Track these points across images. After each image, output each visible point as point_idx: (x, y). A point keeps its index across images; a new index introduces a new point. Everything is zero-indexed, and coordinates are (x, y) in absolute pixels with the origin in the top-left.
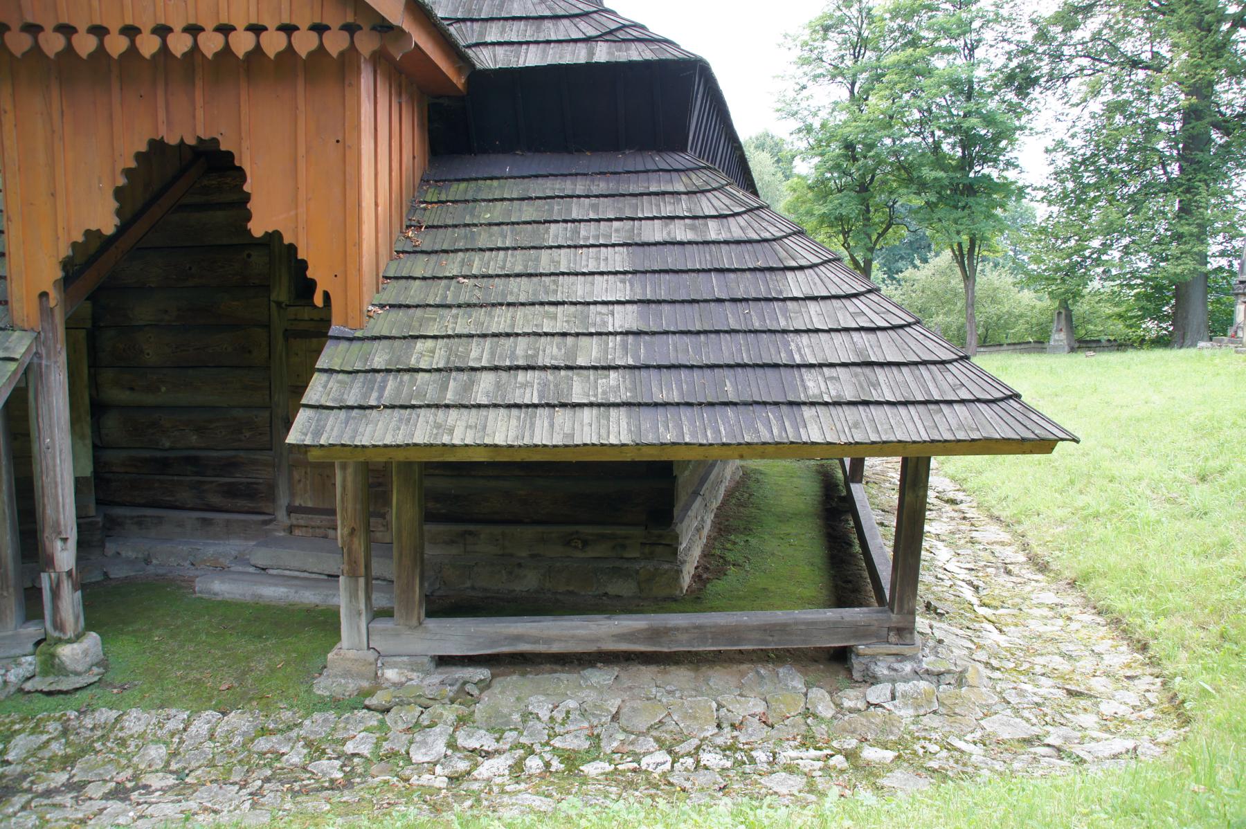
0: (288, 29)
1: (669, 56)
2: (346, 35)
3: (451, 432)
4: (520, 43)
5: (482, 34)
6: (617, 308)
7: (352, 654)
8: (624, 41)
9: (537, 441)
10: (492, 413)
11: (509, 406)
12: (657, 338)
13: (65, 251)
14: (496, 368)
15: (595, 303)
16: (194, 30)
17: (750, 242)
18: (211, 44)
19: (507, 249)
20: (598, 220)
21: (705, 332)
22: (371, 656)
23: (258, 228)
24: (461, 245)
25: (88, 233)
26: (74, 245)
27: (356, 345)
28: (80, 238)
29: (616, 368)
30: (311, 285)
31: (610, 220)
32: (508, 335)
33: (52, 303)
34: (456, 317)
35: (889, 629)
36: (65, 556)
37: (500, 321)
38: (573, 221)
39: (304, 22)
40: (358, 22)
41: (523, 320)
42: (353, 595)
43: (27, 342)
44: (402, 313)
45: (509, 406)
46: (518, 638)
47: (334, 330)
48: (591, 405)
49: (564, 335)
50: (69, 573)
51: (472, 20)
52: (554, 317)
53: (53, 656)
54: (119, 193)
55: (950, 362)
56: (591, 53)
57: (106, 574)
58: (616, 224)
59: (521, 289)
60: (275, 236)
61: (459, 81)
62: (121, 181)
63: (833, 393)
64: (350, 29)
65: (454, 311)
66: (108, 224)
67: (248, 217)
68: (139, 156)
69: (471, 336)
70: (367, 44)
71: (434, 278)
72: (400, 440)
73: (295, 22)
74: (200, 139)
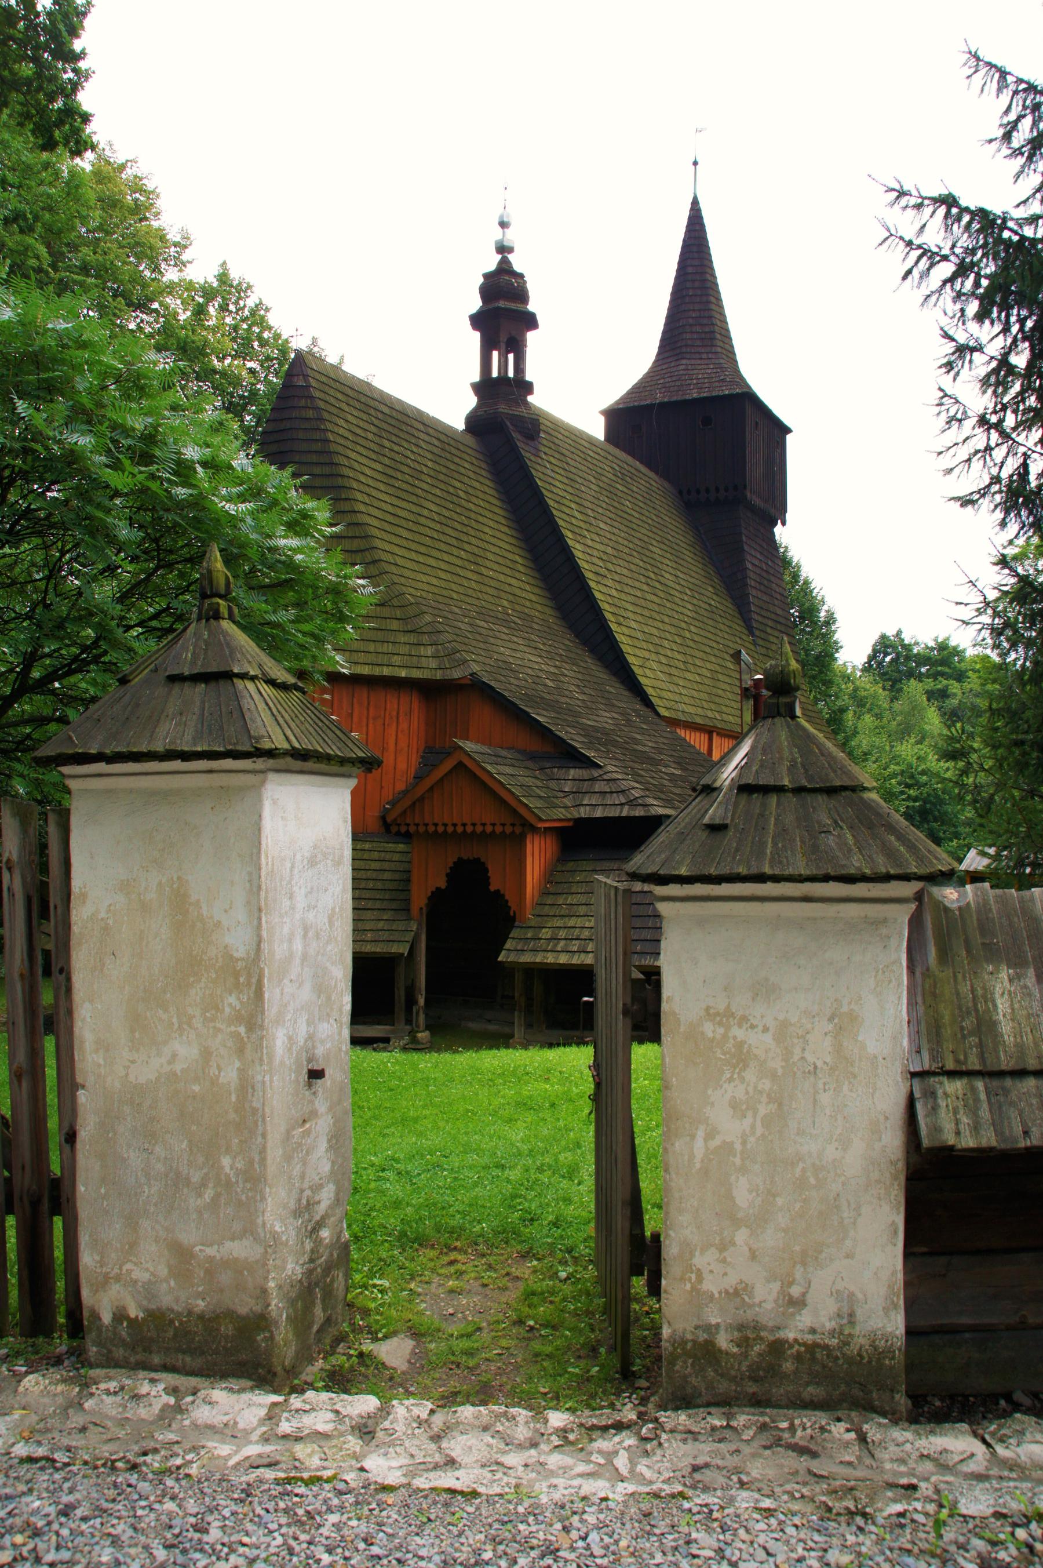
0: (503, 825)
16: (474, 825)
23: (492, 888)
36: (421, 1001)
37: (571, 922)
41: (579, 922)
54: (447, 875)
59: (582, 910)
60: (497, 892)
61: (571, 824)
64: (523, 825)
66: (443, 884)
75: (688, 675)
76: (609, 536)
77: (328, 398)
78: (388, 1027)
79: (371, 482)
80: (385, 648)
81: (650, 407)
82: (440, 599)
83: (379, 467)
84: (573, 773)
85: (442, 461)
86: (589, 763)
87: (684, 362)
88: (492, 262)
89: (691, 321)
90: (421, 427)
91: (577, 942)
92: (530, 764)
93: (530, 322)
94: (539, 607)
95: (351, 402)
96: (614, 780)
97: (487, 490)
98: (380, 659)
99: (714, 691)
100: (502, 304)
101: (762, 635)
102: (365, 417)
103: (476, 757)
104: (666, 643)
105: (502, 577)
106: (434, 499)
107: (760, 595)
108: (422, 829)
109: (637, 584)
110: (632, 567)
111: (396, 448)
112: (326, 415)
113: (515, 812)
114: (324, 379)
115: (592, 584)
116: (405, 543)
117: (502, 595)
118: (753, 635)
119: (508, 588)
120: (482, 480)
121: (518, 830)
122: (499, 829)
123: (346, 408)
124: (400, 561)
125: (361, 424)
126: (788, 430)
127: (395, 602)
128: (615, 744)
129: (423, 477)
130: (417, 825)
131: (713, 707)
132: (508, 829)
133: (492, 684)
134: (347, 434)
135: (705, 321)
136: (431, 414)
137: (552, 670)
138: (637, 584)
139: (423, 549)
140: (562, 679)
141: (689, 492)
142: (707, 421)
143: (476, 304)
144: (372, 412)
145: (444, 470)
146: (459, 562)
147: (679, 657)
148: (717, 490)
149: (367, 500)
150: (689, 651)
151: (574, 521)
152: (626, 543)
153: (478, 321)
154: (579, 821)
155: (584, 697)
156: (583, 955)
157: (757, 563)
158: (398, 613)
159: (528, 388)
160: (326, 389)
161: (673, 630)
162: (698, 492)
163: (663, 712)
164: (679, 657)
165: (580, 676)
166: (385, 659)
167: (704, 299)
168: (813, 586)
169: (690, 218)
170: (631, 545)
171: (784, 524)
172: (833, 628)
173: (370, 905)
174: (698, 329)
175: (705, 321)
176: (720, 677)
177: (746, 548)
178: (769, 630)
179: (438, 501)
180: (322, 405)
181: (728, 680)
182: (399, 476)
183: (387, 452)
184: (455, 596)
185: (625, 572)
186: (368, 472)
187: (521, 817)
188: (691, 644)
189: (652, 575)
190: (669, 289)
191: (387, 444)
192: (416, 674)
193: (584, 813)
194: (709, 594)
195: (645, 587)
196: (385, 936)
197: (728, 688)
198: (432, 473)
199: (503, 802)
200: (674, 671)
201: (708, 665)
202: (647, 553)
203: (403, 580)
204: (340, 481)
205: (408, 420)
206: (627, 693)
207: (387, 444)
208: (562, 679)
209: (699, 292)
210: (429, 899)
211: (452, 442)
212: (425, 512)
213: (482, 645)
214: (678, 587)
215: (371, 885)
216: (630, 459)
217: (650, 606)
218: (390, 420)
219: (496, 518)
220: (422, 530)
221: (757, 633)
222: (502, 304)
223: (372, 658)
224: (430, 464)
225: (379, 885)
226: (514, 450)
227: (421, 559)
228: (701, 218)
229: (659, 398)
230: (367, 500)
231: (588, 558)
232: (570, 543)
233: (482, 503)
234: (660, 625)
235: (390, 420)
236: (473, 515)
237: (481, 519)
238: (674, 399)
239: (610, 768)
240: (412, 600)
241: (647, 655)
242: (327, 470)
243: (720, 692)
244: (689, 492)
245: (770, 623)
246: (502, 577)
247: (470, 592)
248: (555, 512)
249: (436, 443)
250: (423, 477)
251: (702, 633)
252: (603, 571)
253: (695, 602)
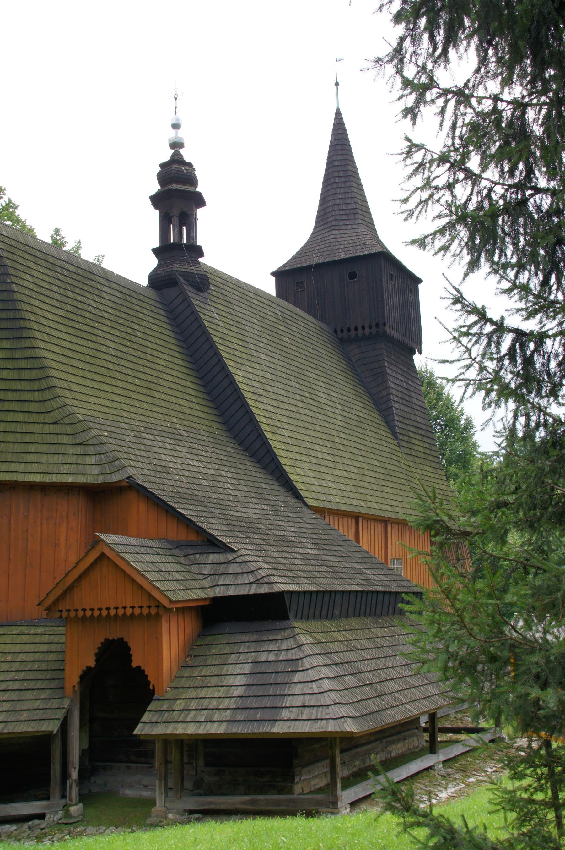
0: (141, 607)
1: (273, 591)
2: (156, 608)
3: (177, 730)
4: (229, 585)
5: (218, 581)
6: (240, 687)
7: (159, 809)
8: (262, 583)
9: (199, 733)
10: (190, 724)
11: (196, 722)
12: (246, 699)
13: (80, 673)
14: (196, 710)
15: (234, 686)
16: (117, 608)
17: (292, 660)
18: (121, 612)
19: (215, 665)
20: (248, 652)
21: (261, 696)
22: (165, 809)
23: (134, 665)
24: (202, 664)
25: (87, 667)
26: (83, 671)
27: (160, 702)
28: (85, 668)
29: (230, 709)
30: (149, 682)
31: (251, 652)
32: (204, 698)
33: (76, 689)
34: (191, 692)
35: (330, 802)
36: (74, 774)
37: (203, 693)
38: (240, 653)
39: (145, 605)
42: (160, 787)
43: (69, 702)
44: (176, 690)
45: (196, 722)
46: (210, 803)
47: (156, 696)
48: (218, 721)
49: (220, 697)
50: (75, 780)
51: (216, 574)
52: (219, 691)
53: (68, 810)
54: (96, 655)
55: (331, 705)
56: (250, 590)
57: (90, 790)
58: (253, 654)
59: (214, 681)
60: (139, 668)
61: (207, 603)
63: (288, 716)
64: (157, 607)
65: (192, 689)
67: (131, 661)
68: (102, 643)
69: (193, 698)
70: (161, 611)
71: (190, 677)
72: (163, 732)
73: (143, 605)
75: (336, 472)
76: (268, 364)
77: (15, 258)
78: (44, 803)
79: (52, 324)
80: (56, 459)
81: (308, 268)
82: (110, 417)
83: (62, 313)
84: (213, 558)
85: (123, 309)
86: (225, 549)
87: (334, 232)
88: (167, 155)
89: (338, 201)
90: (105, 283)
91: (205, 712)
92: (177, 552)
93: (199, 201)
94: (207, 423)
95: (39, 262)
96: (245, 562)
97: (164, 331)
98: (51, 468)
99: (361, 484)
100: (174, 186)
101: (406, 439)
102: (50, 273)
103: (116, 548)
104: (317, 447)
105: (173, 399)
106: (113, 338)
107: (402, 407)
108: (73, 614)
109: (292, 401)
110: (289, 388)
111: (79, 298)
112: (12, 271)
113: (150, 595)
114: (13, 243)
115: (250, 402)
116: (81, 373)
117: (172, 413)
118: (396, 438)
119: (178, 408)
120: (159, 323)
121: (153, 611)
122: (137, 611)
123: (34, 266)
124: (74, 387)
125: (47, 279)
126: (419, 281)
127: (66, 421)
128: (256, 531)
129: (103, 321)
130: (68, 611)
131: (358, 496)
132: (145, 611)
133: (145, 485)
134: (31, 286)
135: (349, 201)
136: (116, 271)
137: (210, 472)
138: (292, 401)
139: (98, 378)
140: (219, 479)
141: (342, 331)
142: (352, 276)
143: (155, 187)
144: (59, 270)
145: (124, 316)
146: (133, 388)
147: (329, 458)
148: (363, 328)
149: (46, 338)
150: (337, 453)
151: (237, 353)
152: (284, 370)
153: (156, 200)
154: (215, 600)
155: (237, 493)
156: (209, 724)
157: (398, 382)
158: (69, 430)
159: (199, 252)
160: (15, 251)
161: (324, 436)
162: (349, 330)
163: (310, 502)
164: (329, 458)
165: (237, 476)
166: (55, 469)
167: (348, 184)
168: (453, 400)
169: (334, 125)
170: (288, 372)
171: (420, 352)
172: (472, 432)
173: (32, 685)
174: (344, 207)
175: (349, 201)
176: (366, 472)
177: (388, 371)
178: (411, 434)
179: (116, 339)
180: (9, 263)
181: (374, 475)
182: (80, 319)
183: (70, 301)
184: (125, 414)
185: (282, 392)
186: (49, 316)
187: (155, 599)
188: (341, 447)
189: (307, 395)
190: (321, 179)
191: (70, 294)
192: (81, 479)
193: (219, 592)
194: (359, 408)
195: (300, 404)
196: (38, 714)
197: (373, 481)
198: (112, 318)
199: (141, 588)
200: (322, 469)
201: (356, 464)
202: (303, 377)
203: (75, 403)
204: (22, 324)
205: (93, 277)
206: (280, 489)
207: (70, 294)
208: (219, 479)
209: (343, 179)
210: (82, 677)
211: (134, 294)
212: (103, 348)
213: (144, 454)
214: (330, 403)
215: (36, 666)
216: (291, 307)
217: (303, 418)
218: (75, 276)
219: (171, 353)
220: (99, 362)
221: (401, 437)
222: (174, 186)
223: (44, 468)
224: (111, 311)
225: (44, 666)
226: (186, 299)
227: (96, 385)
228: (343, 124)
229: (316, 260)
230: (46, 338)
231: (248, 382)
232: (232, 370)
233: (158, 341)
234: (312, 433)
235: (75, 276)
236: (149, 351)
237: (156, 354)
238: (327, 260)
239: (242, 552)
240: (81, 418)
241: (298, 457)
242: (11, 315)
243: (366, 485)
244: (342, 331)
245: (412, 429)
246: (173, 399)
247: (140, 411)
248: (219, 346)
249: (118, 294)
250: (103, 321)
251: (351, 438)
252: (261, 392)
253: (345, 414)
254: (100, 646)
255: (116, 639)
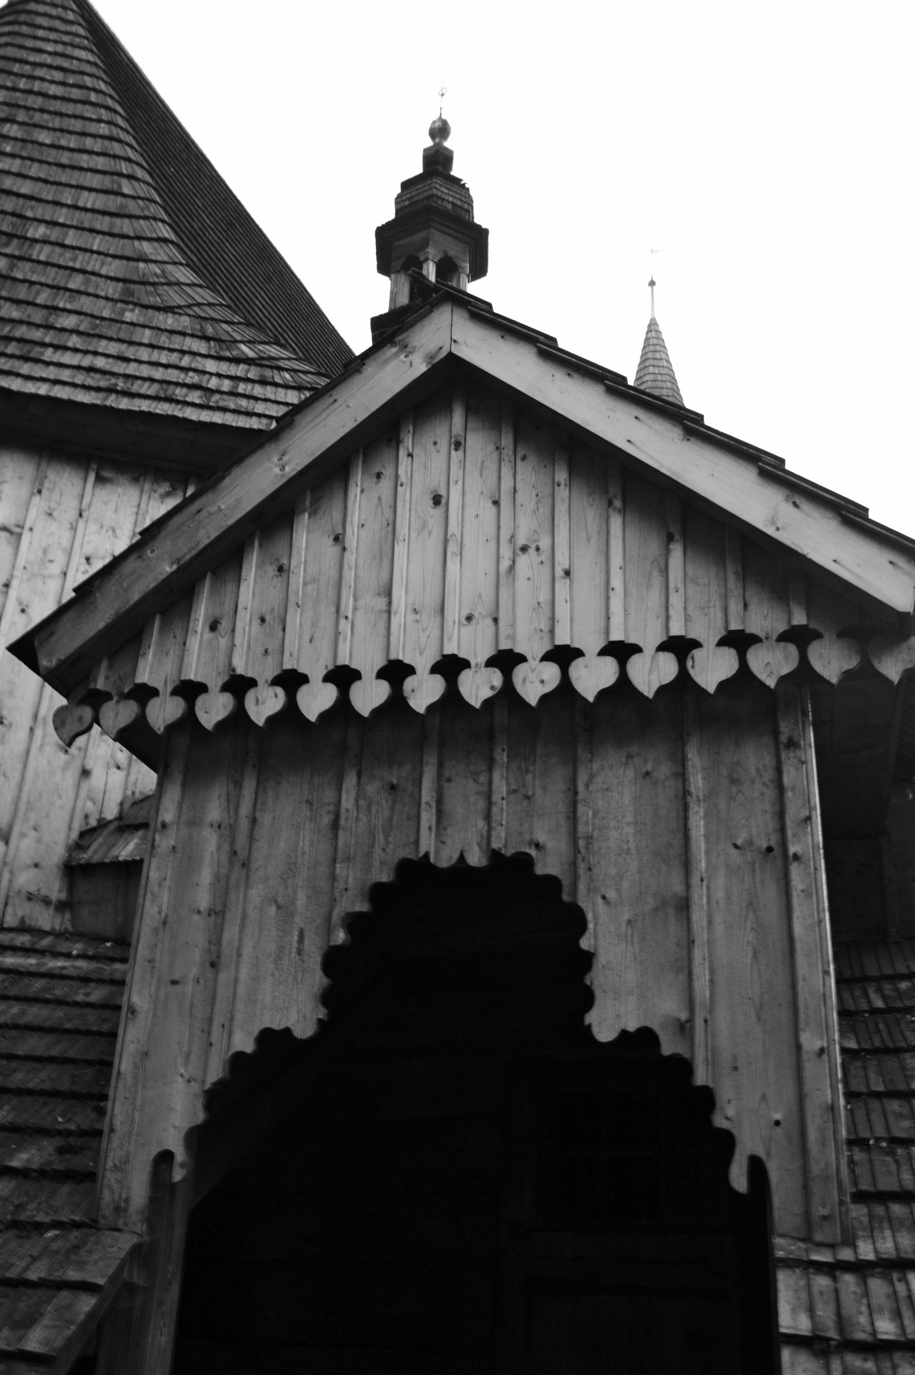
2: (792, 649)
13: (216, 1072)
30: (727, 1141)
33: (178, 1175)
40: (812, 626)
62: (340, 936)
67: (587, 999)
68: (377, 892)
74: (495, 856)
254: (362, 907)
255: (476, 858)
